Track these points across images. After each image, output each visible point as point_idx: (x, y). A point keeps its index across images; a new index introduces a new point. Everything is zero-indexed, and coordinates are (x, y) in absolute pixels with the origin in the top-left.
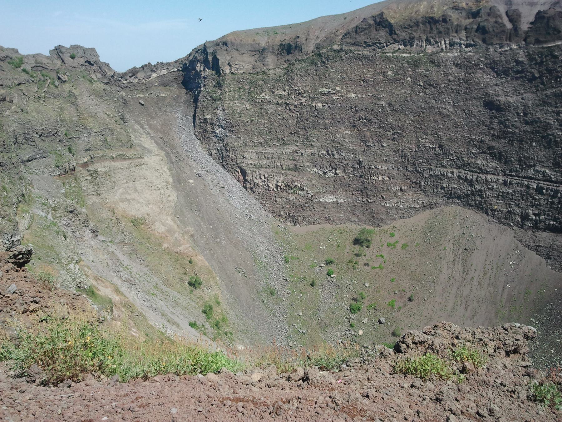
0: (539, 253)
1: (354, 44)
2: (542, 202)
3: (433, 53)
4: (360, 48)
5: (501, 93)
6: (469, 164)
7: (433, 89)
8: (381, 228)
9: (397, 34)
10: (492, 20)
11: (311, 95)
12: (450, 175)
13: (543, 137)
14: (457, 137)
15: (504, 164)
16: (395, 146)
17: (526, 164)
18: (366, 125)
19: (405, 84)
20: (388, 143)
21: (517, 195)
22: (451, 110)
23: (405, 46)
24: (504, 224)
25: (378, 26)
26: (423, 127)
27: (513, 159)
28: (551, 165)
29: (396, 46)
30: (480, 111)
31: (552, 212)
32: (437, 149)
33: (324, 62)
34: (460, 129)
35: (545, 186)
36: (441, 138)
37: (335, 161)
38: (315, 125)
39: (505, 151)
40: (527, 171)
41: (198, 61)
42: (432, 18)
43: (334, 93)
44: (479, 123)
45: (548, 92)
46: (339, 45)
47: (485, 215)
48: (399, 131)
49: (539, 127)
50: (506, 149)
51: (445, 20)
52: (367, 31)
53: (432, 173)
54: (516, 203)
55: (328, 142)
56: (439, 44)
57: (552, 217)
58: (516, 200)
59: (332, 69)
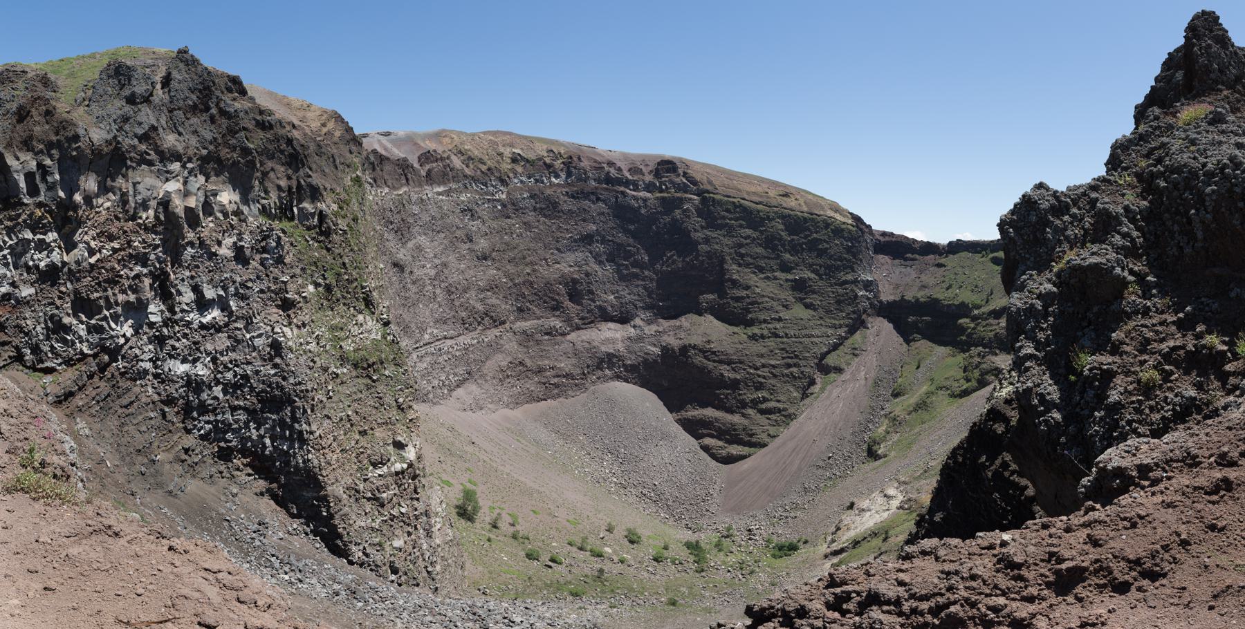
45: (410, 245)
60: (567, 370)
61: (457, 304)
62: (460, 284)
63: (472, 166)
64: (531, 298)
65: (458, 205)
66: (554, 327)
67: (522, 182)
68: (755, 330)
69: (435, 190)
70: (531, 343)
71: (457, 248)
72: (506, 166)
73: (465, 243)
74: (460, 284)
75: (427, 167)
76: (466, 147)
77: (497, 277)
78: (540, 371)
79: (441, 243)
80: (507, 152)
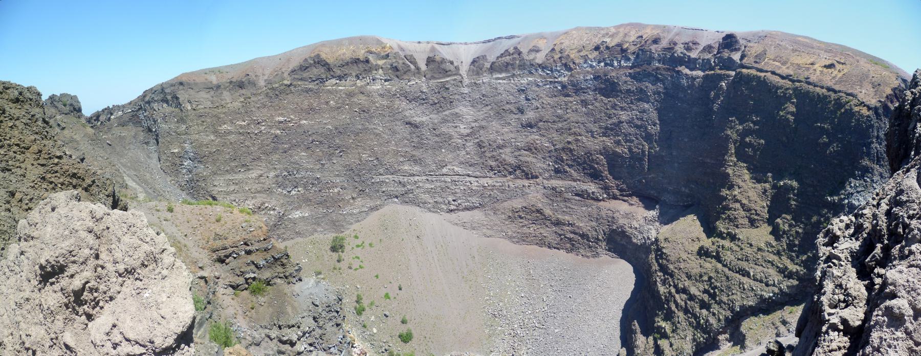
1: (301, 79)
2: (456, 190)
3: (362, 87)
4: (306, 83)
5: (414, 115)
8: (344, 233)
10: (401, 62)
11: (269, 124)
12: (387, 180)
14: (388, 151)
20: (337, 160)
22: (381, 129)
23: (340, 81)
24: (433, 212)
26: (363, 145)
29: (334, 81)
32: (375, 162)
35: (457, 180)
37: (297, 180)
38: (275, 149)
41: (155, 101)
42: (358, 59)
43: (289, 121)
45: (447, 113)
50: (423, 156)
51: (367, 61)
52: (309, 69)
59: (285, 100)
60: (585, 230)
61: (488, 154)
64: (570, 162)
66: (587, 190)
67: (591, 66)
68: (707, 243)
69: (494, 77)
70: (559, 199)
71: (503, 117)
74: (495, 142)
77: (538, 142)
78: (558, 223)
79: (486, 113)
80: (597, 41)
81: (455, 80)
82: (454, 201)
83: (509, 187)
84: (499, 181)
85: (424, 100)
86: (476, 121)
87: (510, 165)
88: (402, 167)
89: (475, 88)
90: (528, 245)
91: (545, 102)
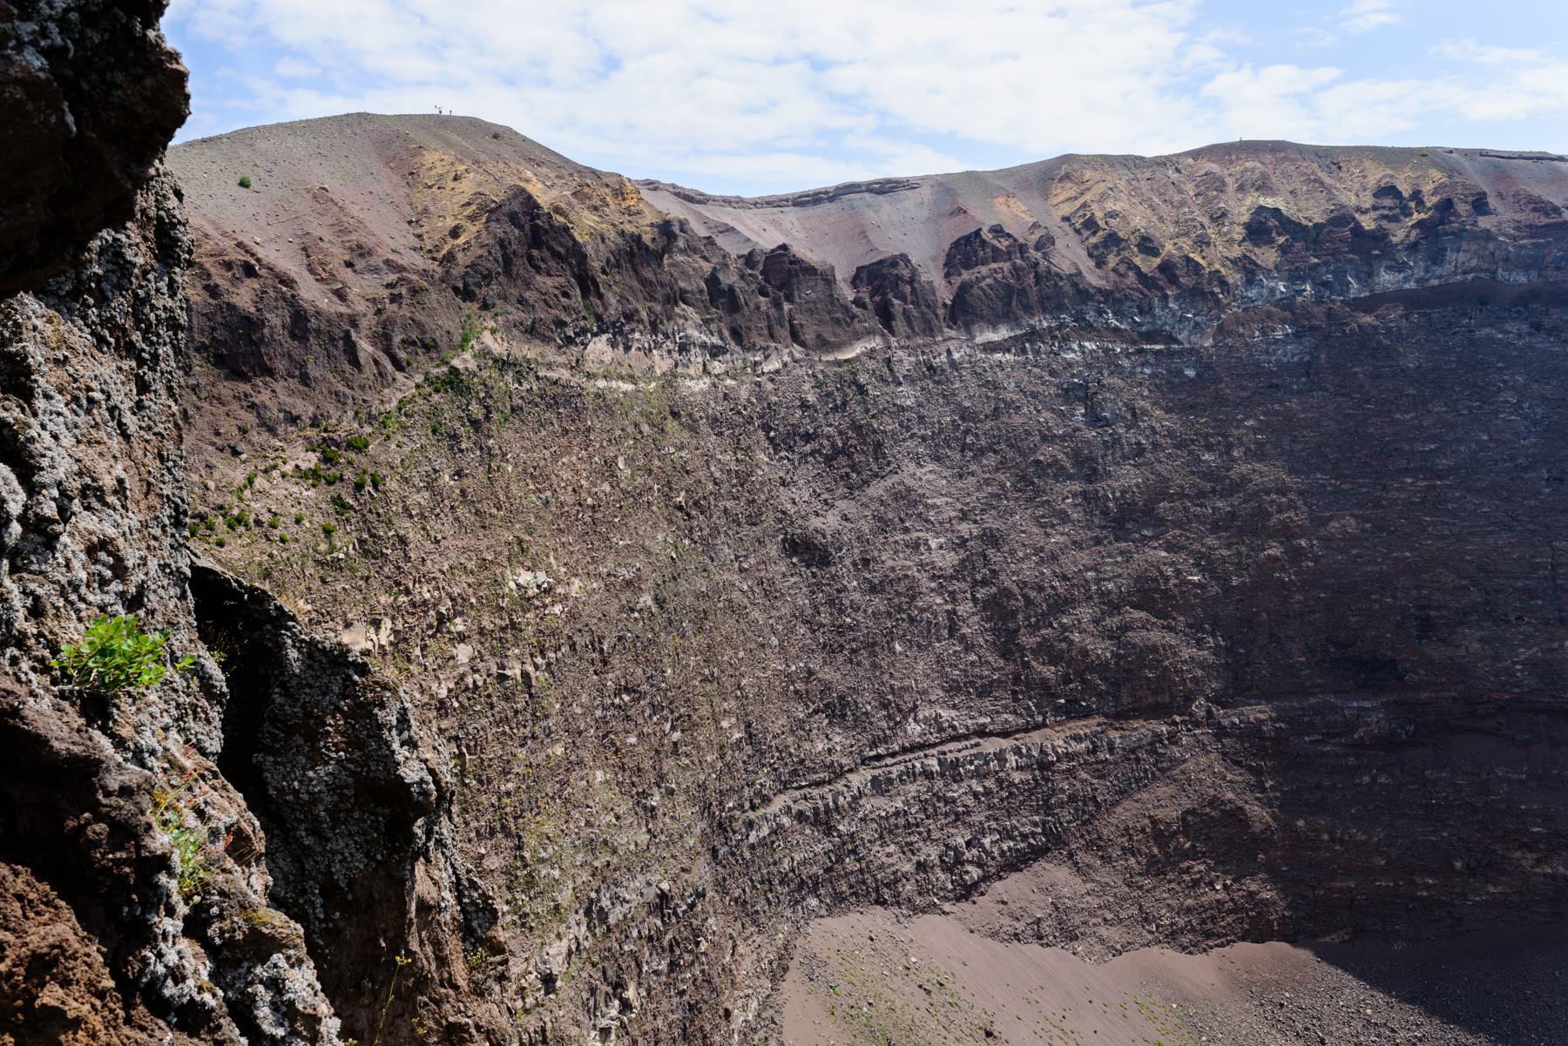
0: (1045, 941)
1: (532, 332)
4: (551, 354)
6: (802, 762)
7: (701, 517)
9: (600, 296)
13: (912, 620)
15: (853, 729)
16: (688, 774)
17: (900, 711)
18: (628, 718)
19: (654, 508)
21: (913, 811)
24: (924, 911)
25: (535, 252)
27: (869, 708)
28: (941, 694)
30: (784, 575)
31: (996, 819)
33: (475, 424)
34: (768, 651)
35: (960, 755)
36: (747, 698)
39: (849, 688)
40: (906, 732)
44: (794, 616)
45: (877, 489)
46: (493, 332)
47: (878, 907)
48: (682, 710)
49: (898, 594)
50: (851, 681)
53: (752, 839)
54: (920, 833)
55: (580, 858)
56: (668, 343)
57: (999, 833)
58: (917, 825)
61: (1028, 640)
62: (1041, 589)
63: (1112, 261)
65: (1052, 373)
69: (980, 339)
71: (1039, 492)
72: (1221, 254)
73: (1070, 477)
74: (1041, 589)
75: (966, 275)
76: (1110, 206)
77: (1169, 571)
80: (1242, 208)
81: (871, 354)
82: (969, 844)
83: (1111, 749)
84: (1082, 732)
85: (808, 437)
86: (964, 516)
87: (1102, 668)
88: (807, 746)
89: (931, 385)
90: (1222, 945)
91: (1157, 426)
